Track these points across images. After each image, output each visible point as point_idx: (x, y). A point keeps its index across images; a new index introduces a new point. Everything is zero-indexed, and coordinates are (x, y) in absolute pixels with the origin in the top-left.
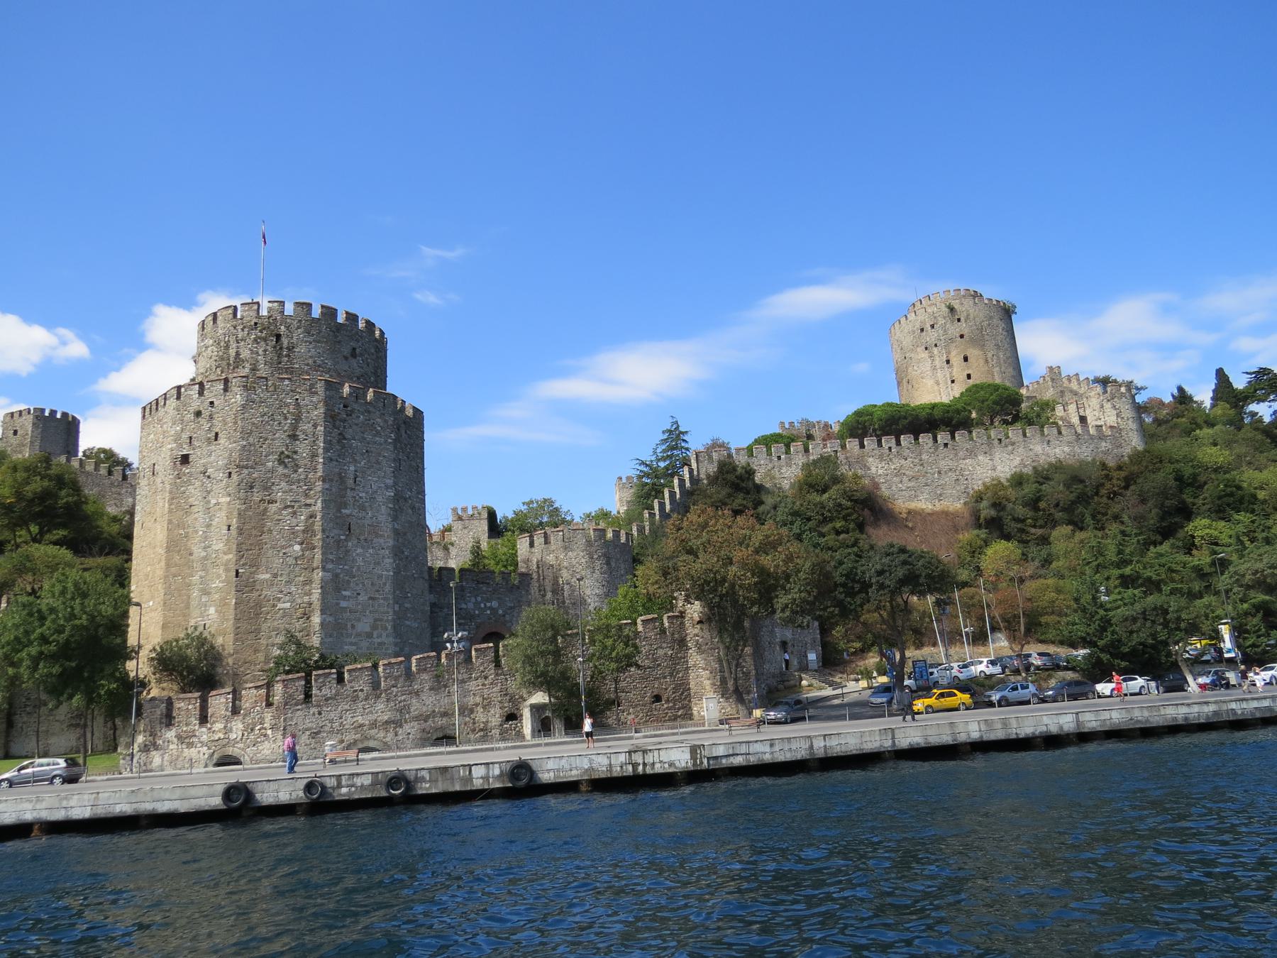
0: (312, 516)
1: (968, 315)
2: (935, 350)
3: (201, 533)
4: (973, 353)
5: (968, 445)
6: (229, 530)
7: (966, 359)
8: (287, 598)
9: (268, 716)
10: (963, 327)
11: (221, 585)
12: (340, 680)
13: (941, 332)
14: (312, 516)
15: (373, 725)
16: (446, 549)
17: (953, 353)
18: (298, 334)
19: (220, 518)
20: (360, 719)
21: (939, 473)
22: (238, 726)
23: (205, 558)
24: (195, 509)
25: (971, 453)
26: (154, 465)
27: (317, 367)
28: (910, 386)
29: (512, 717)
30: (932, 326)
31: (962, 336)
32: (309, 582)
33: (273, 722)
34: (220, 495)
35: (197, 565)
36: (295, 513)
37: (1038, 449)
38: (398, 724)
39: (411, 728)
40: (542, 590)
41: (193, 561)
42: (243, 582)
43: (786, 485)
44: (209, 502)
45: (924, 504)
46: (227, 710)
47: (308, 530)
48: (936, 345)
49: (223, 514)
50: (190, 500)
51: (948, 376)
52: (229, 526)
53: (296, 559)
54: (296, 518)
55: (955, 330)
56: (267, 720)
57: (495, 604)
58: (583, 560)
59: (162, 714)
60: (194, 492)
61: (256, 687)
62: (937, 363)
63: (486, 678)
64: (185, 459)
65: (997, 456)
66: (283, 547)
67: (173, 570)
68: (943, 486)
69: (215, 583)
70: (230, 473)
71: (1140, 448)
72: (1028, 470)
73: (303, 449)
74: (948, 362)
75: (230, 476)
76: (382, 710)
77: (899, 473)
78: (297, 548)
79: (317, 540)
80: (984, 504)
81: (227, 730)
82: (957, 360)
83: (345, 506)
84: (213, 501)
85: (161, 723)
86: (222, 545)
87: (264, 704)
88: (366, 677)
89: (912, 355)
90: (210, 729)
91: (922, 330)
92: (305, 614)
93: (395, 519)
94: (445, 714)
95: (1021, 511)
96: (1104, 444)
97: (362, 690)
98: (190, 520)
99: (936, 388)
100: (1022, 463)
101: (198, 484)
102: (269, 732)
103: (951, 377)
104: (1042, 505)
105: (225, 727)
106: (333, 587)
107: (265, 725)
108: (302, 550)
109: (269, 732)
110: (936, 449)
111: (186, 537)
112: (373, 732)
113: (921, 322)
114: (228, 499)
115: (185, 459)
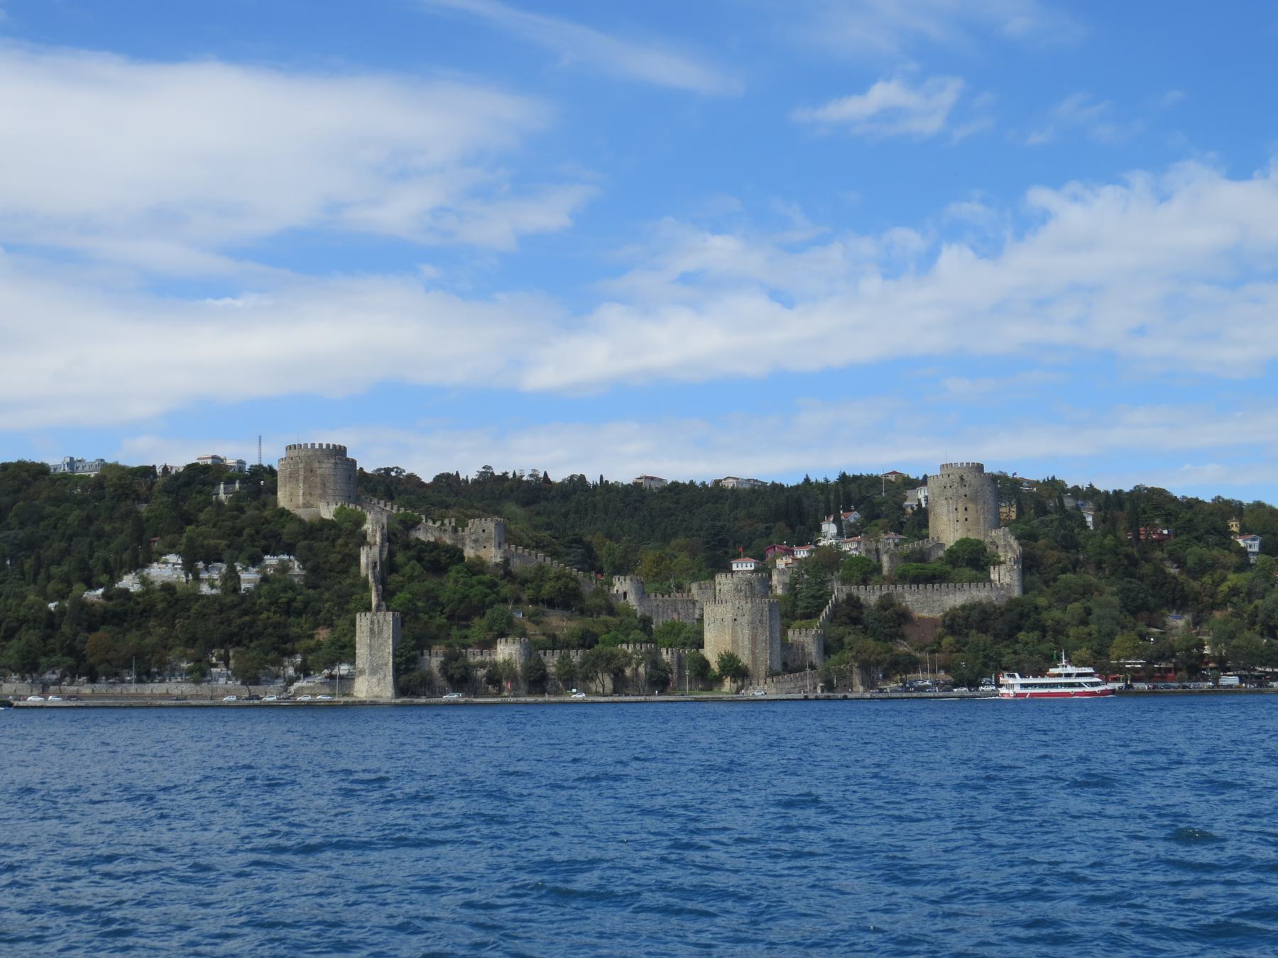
4: (970, 506)
5: (947, 590)
7: (966, 509)
10: (967, 490)
16: (694, 604)
17: (960, 505)
18: (756, 583)
19: (746, 636)
22: (766, 686)
25: (947, 594)
29: (815, 688)
31: (965, 496)
37: (975, 593)
40: (798, 649)
42: (753, 653)
43: (872, 603)
45: (925, 614)
55: (962, 491)
62: (951, 508)
64: (735, 620)
65: (957, 595)
68: (934, 607)
71: (1016, 592)
72: (968, 604)
74: (956, 509)
76: (792, 685)
77: (917, 601)
80: (947, 618)
82: (961, 509)
95: (961, 621)
100: (967, 599)
104: (970, 620)
106: (771, 654)
115: (735, 620)
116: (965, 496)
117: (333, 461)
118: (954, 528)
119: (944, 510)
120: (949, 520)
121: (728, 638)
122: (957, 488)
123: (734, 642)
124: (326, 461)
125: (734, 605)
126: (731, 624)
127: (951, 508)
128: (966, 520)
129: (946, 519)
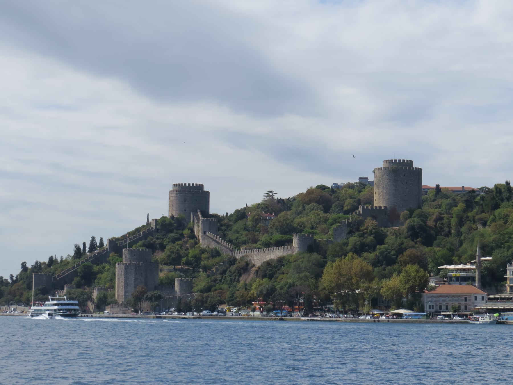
12: (115, 306)
15: (118, 311)
18: (127, 254)
20: (117, 310)
27: (129, 259)
38: (120, 311)
39: (121, 312)
57: (168, 292)
73: (122, 273)
76: (118, 309)
79: (124, 286)
83: (127, 281)
88: (117, 305)
93: (135, 282)
96: (289, 252)
106: (125, 292)
117: (175, 192)
124: (173, 193)
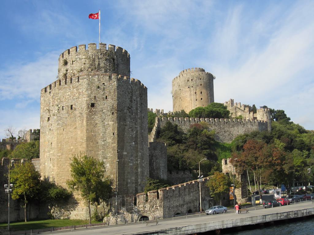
0: (137, 132)
1: (204, 78)
2: (192, 88)
3: (101, 135)
6: (114, 134)
7: (201, 93)
8: (132, 162)
9: (158, 202)
11: (111, 155)
13: (195, 82)
14: (137, 132)
21: (225, 131)
22: (148, 206)
23: (104, 145)
24: (98, 125)
26: (72, 106)
28: (181, 100)
30: (192, 80)
32: (137, 156)
33: (160, 204)
34: (109, 121)
35: (101, 148)
36: (132, 130)
41: (99, 146)
44: (105, 123)
46: (144, 200)
47: (136, 137)
48: (192, 87)
49: (111, 128)
50: (96, 121)
51: (195, 98)
52: (114, 133)
53: (133, 147)
54: (133, 132)
56: (158, 204)
58: (160, 154)
59: (121, 202)
60: (97, 119)
61: (154, 192)
62: (192, 93)
63: (196, 191)
64: (93, 105)
66: (130, 143)
67: (90, 149)
69: (109, 154)
70: (113, 113)
74: (195, 93)
75: (113, 114)
78: (134, 143)
81: (145, 207)
82: (198, 93)
84: (106, 123)
85: (120, 205)
86: (111, 140)
87: (157, 198)
89: (183, 89)
90: (138, 207)
91: (188, 81)
92: (136, 168)
94: (190, 203)
97: (177, 194)
98: (96, 129)
99: (191, 101)
101: (99, 115)
102: (158, 208)
103: (196, 98)
105: (144, 206)
107: (157, 205)
108: (135, 144)
109: (158, 208)
110: (224, 124)
111: (95, 136)
112: (179, 208)
113: (188, 78)
114: (113, 123)
115: (93, 105)
116: (201, 85)
118: (194, 104)
119: (188, 94)
120: (191, 100)
121: (81, 134)
122: (196, 80)
123: (91, 139)
125: (90, 84)
126: (85, 112)
127: (192, 93)
128: (202, 99)
129: (189, 99)
